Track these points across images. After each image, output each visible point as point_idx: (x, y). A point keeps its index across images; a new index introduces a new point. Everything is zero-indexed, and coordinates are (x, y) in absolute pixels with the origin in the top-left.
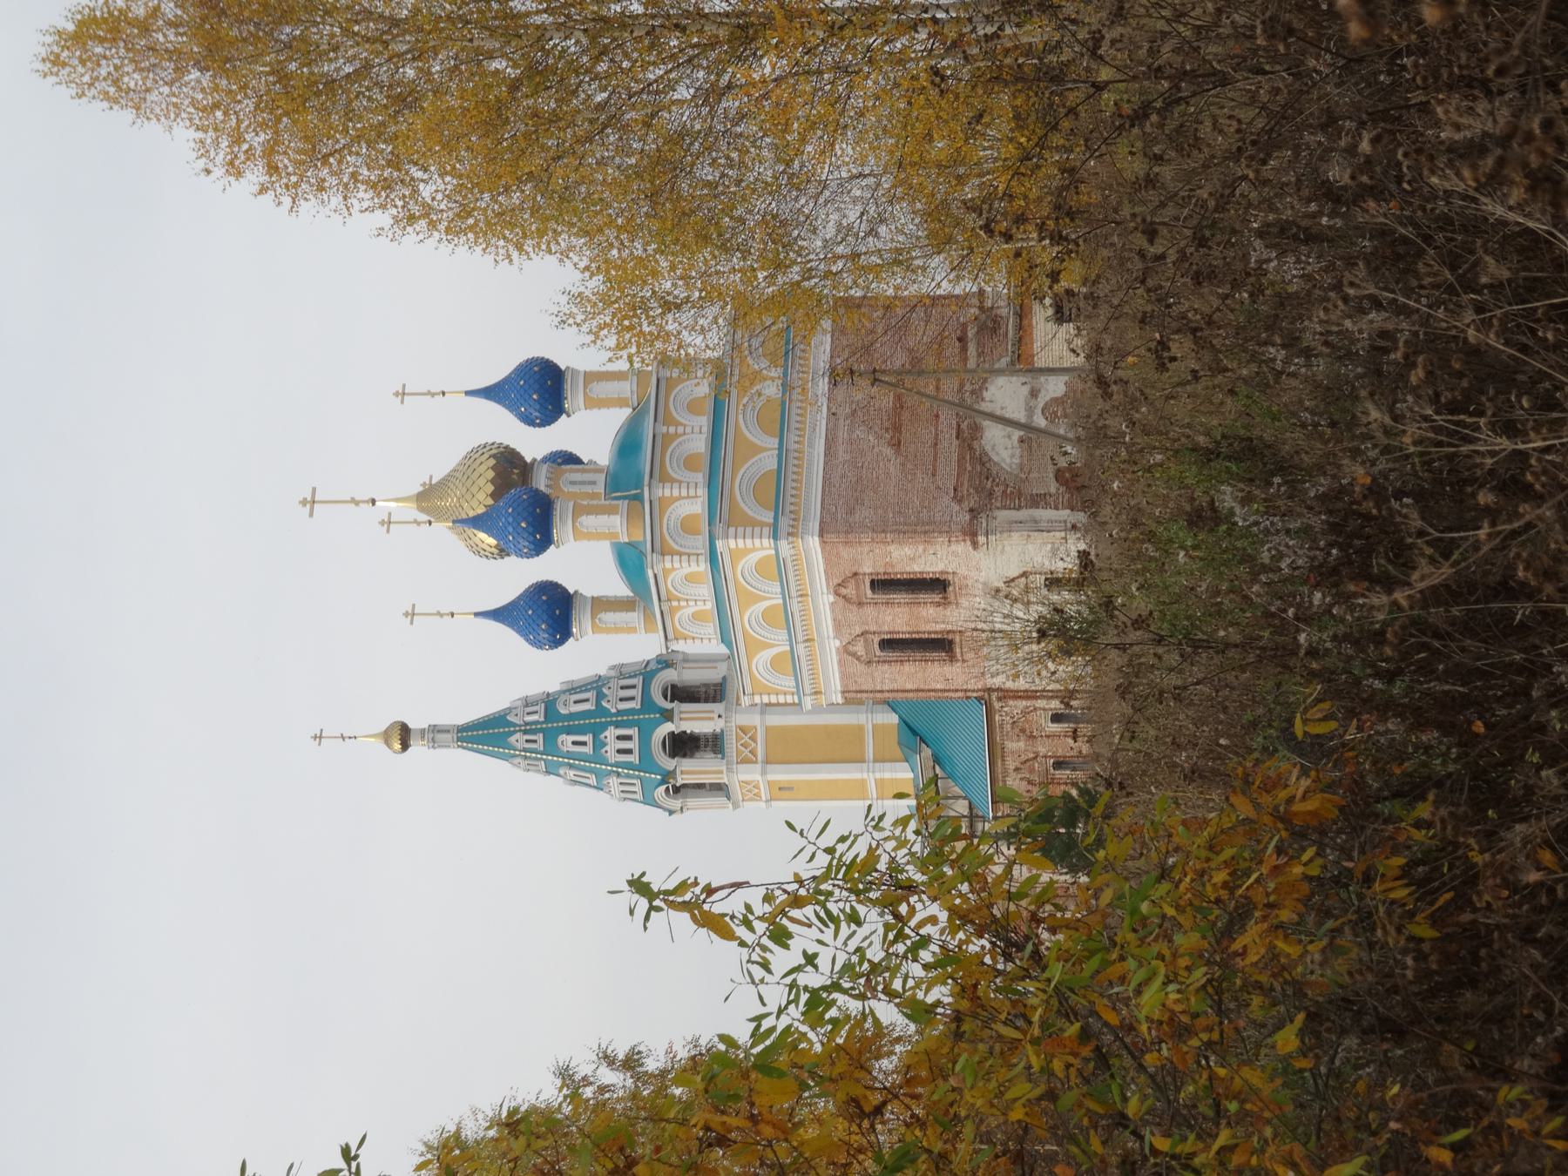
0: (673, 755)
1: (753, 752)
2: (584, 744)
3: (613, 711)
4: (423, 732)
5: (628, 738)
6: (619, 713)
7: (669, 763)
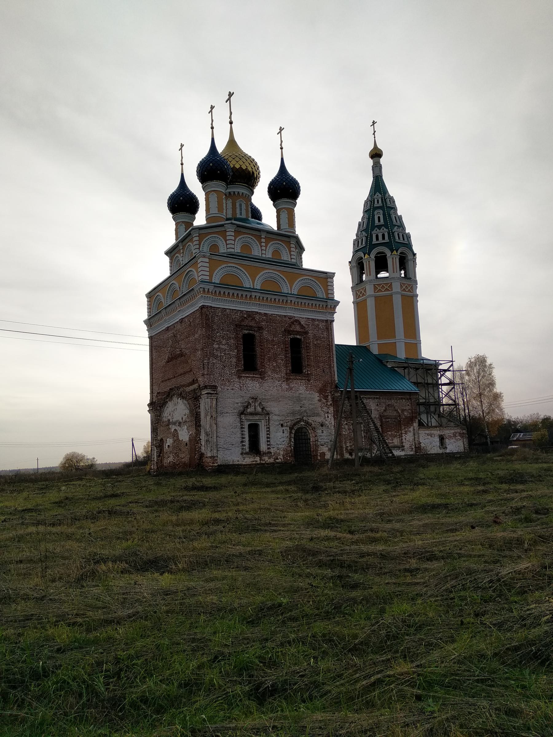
0: (375, 257)
1: (380, 291)
2: (379, 221)
3: (393, 231)
4: (379, 162)
5: (383, 238)
6: (393, 233)
7: (373, 255)
